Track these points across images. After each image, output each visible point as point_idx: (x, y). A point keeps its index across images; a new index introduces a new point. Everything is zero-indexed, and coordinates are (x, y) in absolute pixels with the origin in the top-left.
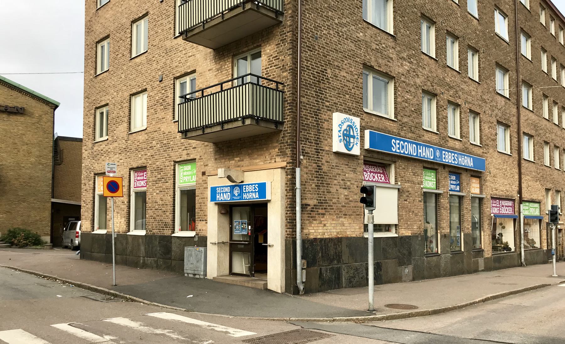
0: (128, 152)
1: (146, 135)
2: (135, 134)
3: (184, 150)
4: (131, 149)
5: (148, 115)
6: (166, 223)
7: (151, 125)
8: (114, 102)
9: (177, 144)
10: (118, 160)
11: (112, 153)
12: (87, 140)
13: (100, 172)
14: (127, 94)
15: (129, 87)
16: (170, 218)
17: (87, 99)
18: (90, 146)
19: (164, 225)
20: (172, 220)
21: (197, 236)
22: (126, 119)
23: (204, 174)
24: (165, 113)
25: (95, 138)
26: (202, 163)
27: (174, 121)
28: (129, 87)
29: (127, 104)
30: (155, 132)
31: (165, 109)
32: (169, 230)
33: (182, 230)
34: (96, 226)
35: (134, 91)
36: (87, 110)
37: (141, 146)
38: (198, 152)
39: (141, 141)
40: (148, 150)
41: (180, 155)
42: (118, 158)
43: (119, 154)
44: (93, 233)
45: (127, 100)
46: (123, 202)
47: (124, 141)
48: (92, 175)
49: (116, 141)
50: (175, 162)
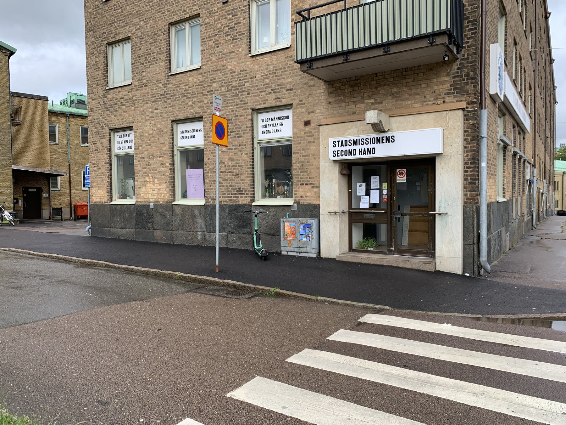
0: (169, 99)
1: (200, 76)
2: (180, 75)
3: (270, 93)
4: (175, 95)
5: (202, 48)
6: (240, 189)
7: (209, 62)
8: (140, 34)
9: (257, 86)
10: (151, 110)
11: (141, 102)
12: (95, 86)
13: (120, 126)
14: (163, 24)
15: (166, 13)
16: (247, 183)
17: (91, 33)
18: (101, 93)
19: (237, 191)
20: (251, 185)
21: (296, 205)
22: (163, 57)
23: (307, 123)
24: (234, 46)
25: (108, 83)
26: (304, 110)
27: (250, 55)
28: (166, 13)
29: (165, 37)
30: (215, 71)
31: (233, 40)
32: (246, 197)
33: (264, 196)
34: (115, 194)
35: (176, 18)
36: (92, 46)
37: (191, 91)
38: (297, 95)
39: (191, 84)
40: (204, 95)
41: (262, 101)
42: (151, 107)
43: (153, 102)
44: (111, 203)
45: (163, 30)
46: (162, 164)
47: (161, 85)
48: (107, 130)
49: (147, 86)
50: (254, 110)
